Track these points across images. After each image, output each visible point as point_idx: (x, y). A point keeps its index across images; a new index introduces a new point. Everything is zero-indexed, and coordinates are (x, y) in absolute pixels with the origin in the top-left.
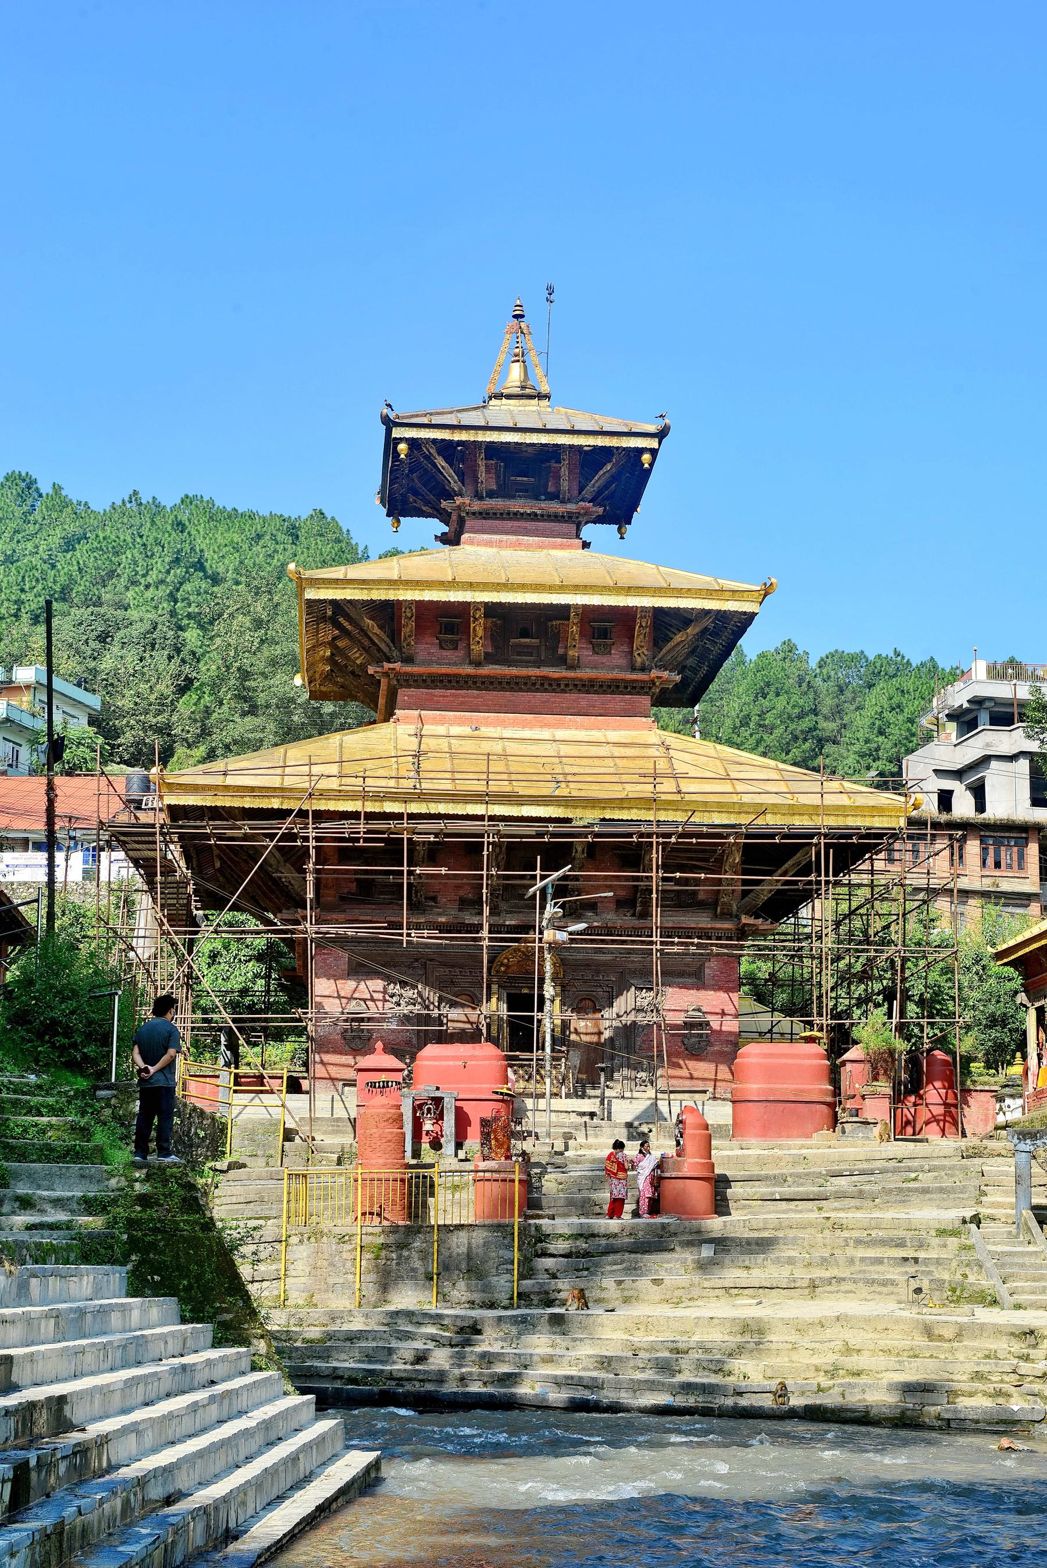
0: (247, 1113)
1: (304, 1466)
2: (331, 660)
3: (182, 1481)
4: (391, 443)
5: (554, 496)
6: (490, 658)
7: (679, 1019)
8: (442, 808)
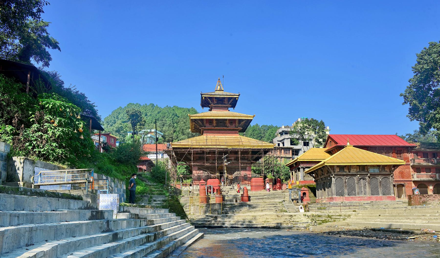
0: (184, 189)
1: (193, 235)
2: (194, 127)
3: (177, 237)
4: (202, 97)
6: (216, 126)
7: (243, 175)
8: (210, 147)
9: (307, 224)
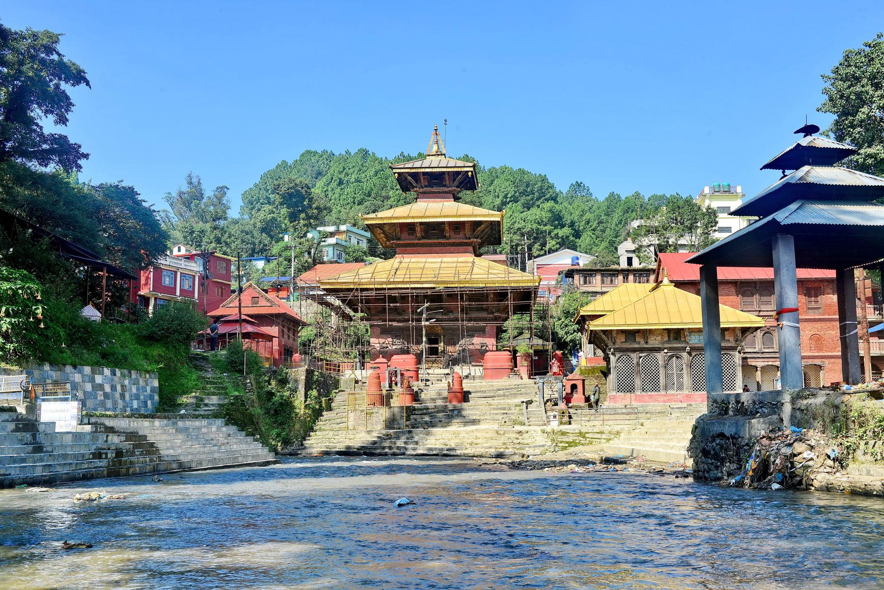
5: (445, 186)
6: (423, 238)
8: (400, 286)
9: (542, 448)
